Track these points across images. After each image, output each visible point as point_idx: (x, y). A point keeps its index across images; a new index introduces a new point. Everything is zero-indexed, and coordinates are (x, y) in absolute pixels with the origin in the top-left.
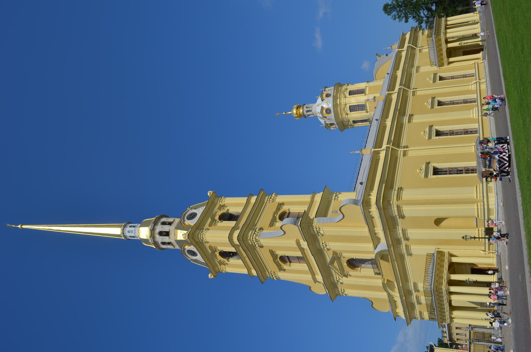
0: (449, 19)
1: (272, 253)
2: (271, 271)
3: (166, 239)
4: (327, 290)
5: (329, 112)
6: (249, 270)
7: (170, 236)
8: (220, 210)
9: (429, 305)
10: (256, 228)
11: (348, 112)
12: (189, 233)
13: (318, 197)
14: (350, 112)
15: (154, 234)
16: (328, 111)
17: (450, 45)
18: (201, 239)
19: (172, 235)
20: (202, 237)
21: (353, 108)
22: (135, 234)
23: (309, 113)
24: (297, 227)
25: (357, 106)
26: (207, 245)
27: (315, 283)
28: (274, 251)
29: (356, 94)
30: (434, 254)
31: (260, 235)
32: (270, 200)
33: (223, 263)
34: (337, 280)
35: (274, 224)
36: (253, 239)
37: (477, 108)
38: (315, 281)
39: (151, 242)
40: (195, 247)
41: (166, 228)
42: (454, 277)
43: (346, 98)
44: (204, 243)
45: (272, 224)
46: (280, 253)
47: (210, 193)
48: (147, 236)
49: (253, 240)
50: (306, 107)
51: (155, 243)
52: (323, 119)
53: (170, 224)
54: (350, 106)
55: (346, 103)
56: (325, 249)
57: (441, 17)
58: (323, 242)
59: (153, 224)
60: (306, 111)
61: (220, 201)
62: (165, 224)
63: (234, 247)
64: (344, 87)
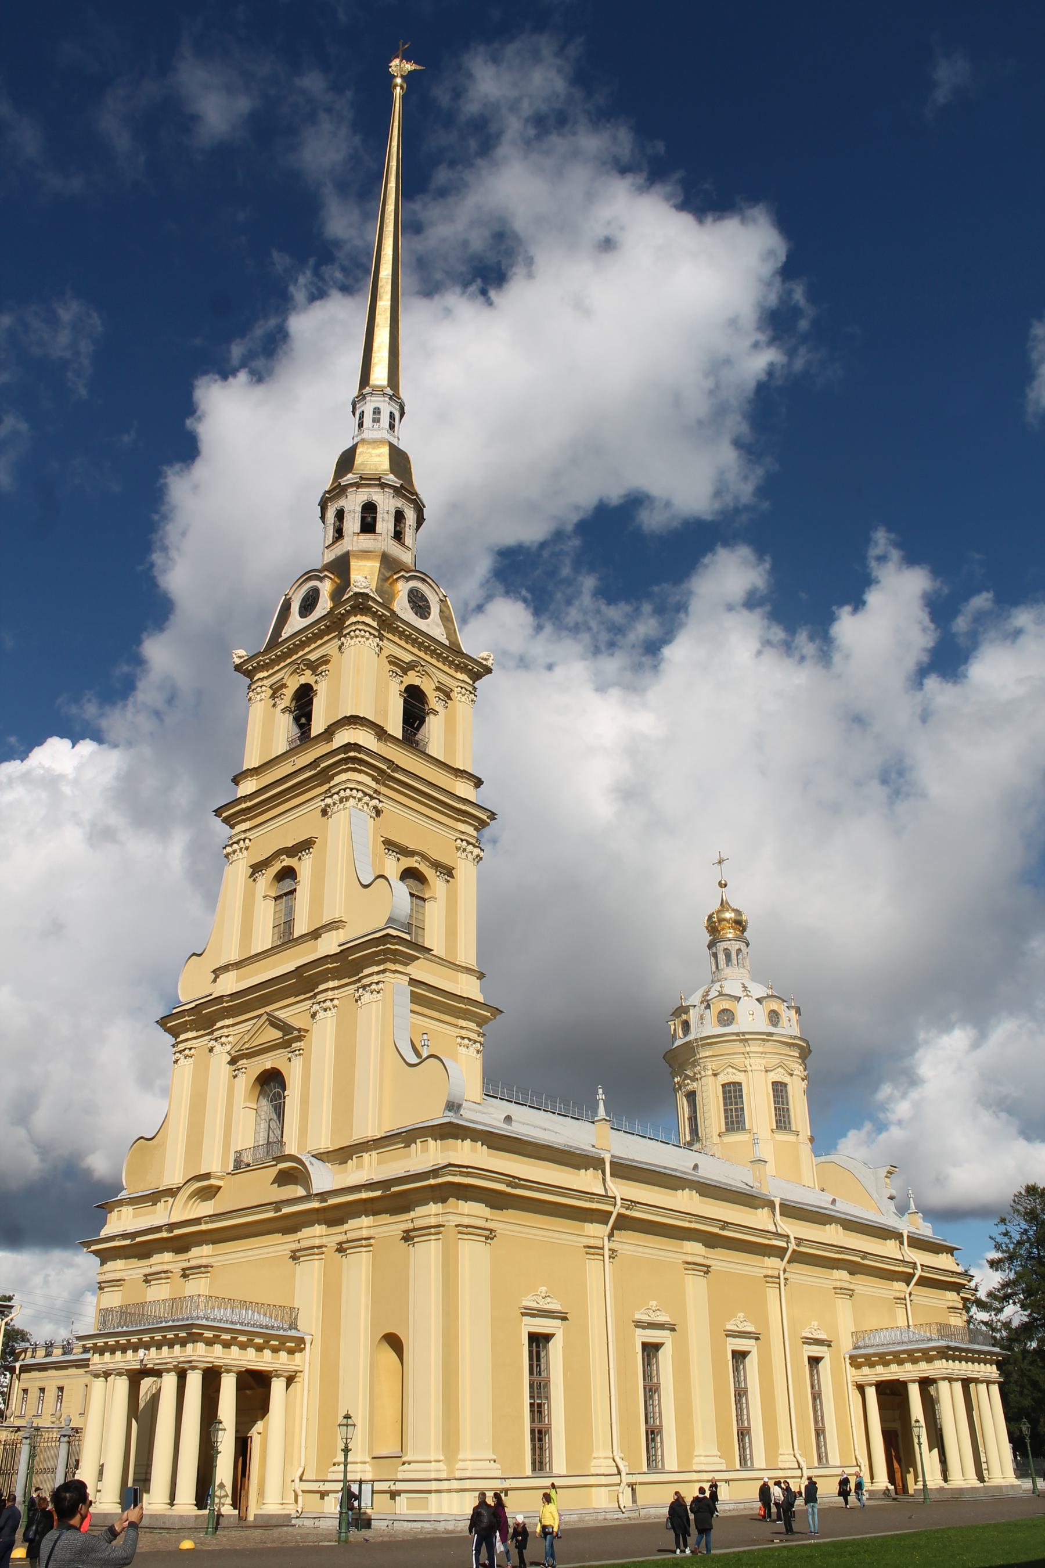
0: (995, 1389)
1: (305, 846)
2: (250, 840)
3: (352, 524)
4: (193, 1005)
5: (724, 1020)
6: (255, 771)
7: (363, 537)
8: (438, 689)
9: (147, 1312)
10: (381, 799)
11: (723, 1079)
12: (371, 597)
13: (469, 987)
14: (723, 1086)
16: (726, 1017)
17: (914, 1391)
18: (352, 634)
19: (366, 542)
20: (357, 637)
21: (733, 1093)
22: (368, 428)
23: (722, 957)
24: (382, 925)
25: (739, 1106)
26: (330, 648)
27: (214, 972)
28: (311, 850)
29: (775, 1103)
30: (296, 1328)
31: (360, 810)
32: (462, 840)
33: (278, 694)
35: (390, 852)
36: (348, 791)
37: (725, 1469)
38: (217, 972)
40: (329, 613)
41: (385, 525)
42: (228, 1386)
43: (763, 1073)
44: (340, 639)
45: (391, 845)
46: (305, 866)
47: (486, 660)
48: (362, 467)
49: (345, 790)
50: (739, 951)
52: (702, 1002)
53: (398, 536)
54: (740, 1084)
55: (750, 1073)
56: (316, 1007)
57: (1000, 1365)
58: (336, 1002)
59: (399, 486)
61: (462, 688)
62: (396, 520)
63: (326, 731)
64: (798, 1066)
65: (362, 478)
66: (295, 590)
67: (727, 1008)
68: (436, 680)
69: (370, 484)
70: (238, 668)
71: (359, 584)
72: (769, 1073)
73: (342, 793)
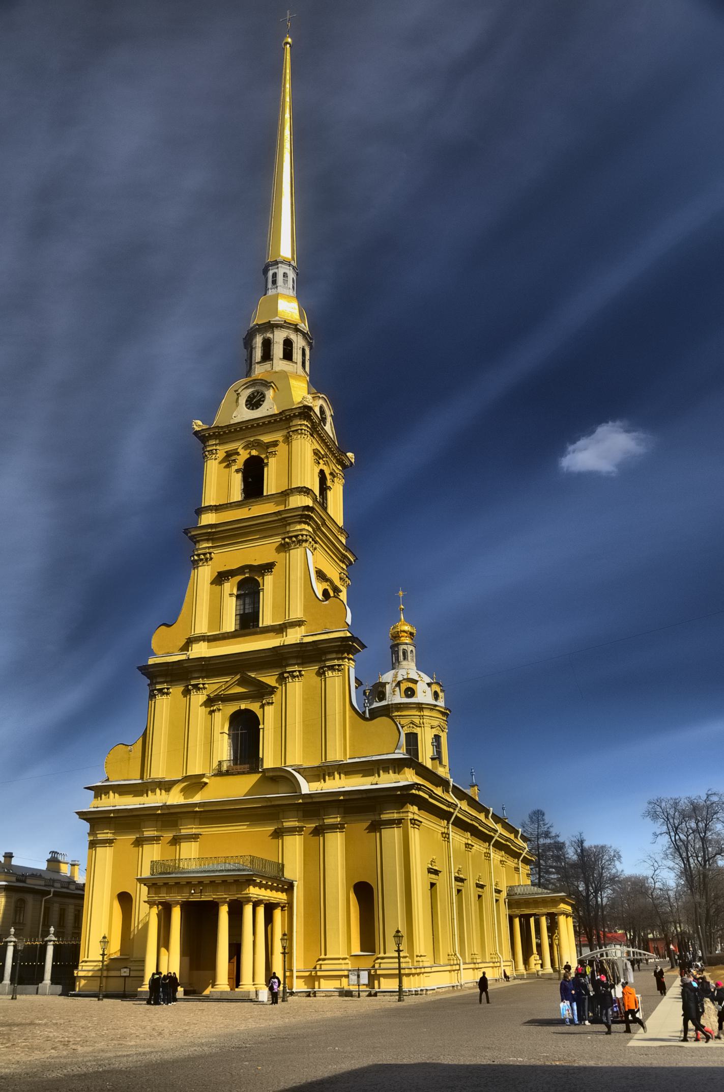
1: (268, 567)
3: (278, 350)
7: (286, 362)
8: (331, 474)
14: (406, 734)
15: (288, 328)
16: (410, 692)
18: (300, 431)
20: (302, 433)
23: (401, 654)
28: (273, 570)
33: (233, 458)
34: (199, 684)
36: (305, 536)
39: (274, 319)
41: (297, 355)
50: (412, 651)
51: (271, 326)
54: (417, 734)
60: (406, 649)
65: (285, 322)
66: (243, 389)
67: (411, 686)
68: (331, 469)
69: (289, 327)
70: (196, 433)
71: (308, 400)
72: (433, 729)
73: (300, 537)
